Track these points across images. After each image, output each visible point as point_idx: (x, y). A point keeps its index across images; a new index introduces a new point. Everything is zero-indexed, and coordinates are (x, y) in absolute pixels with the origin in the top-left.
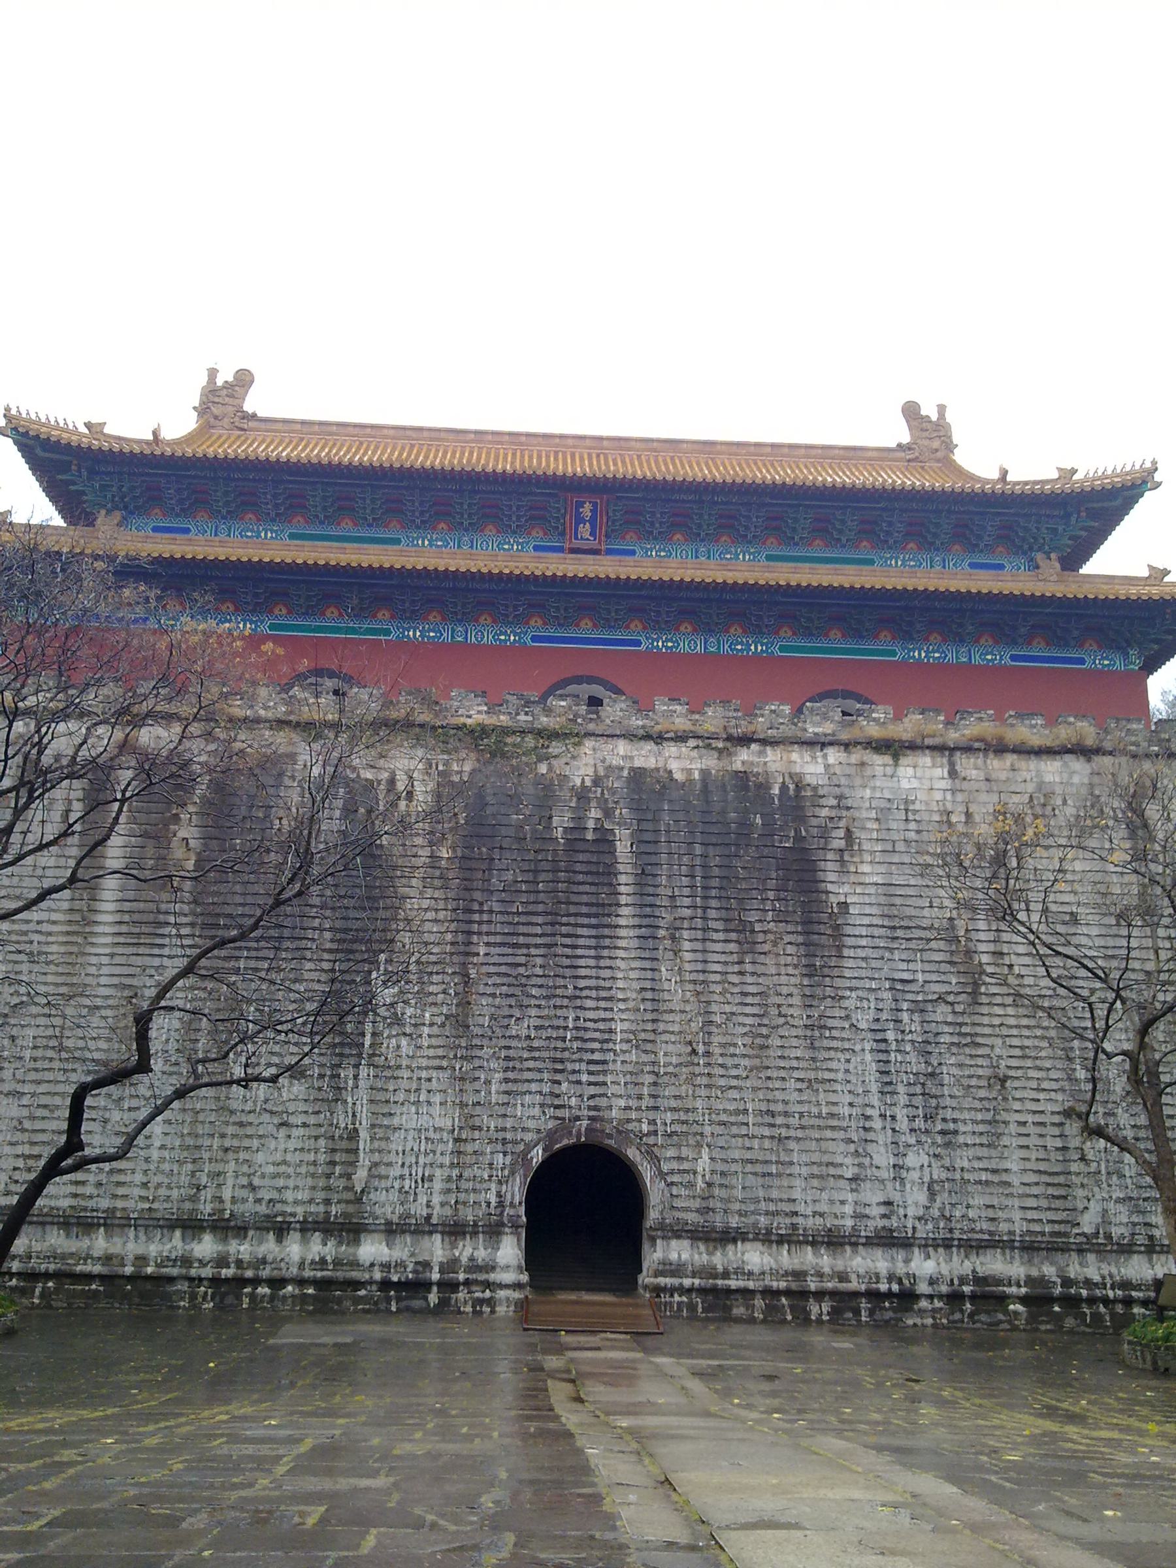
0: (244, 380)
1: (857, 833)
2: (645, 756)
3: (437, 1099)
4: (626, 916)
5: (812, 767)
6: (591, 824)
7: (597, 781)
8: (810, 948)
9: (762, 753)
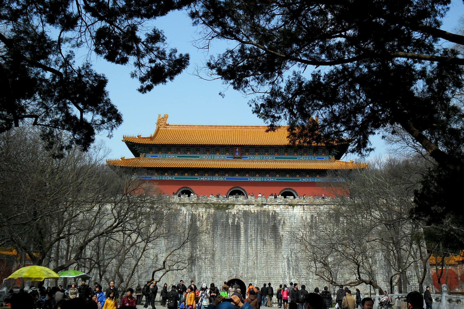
0: (166, 117)
1: (286, 222)
2: (246, 208)
3: (209, 271)
4: (242, 238)
5: (277, 209)
6: (236, 221)
7: (237, 213)
8: (276, 244)
9: (268, 207)
